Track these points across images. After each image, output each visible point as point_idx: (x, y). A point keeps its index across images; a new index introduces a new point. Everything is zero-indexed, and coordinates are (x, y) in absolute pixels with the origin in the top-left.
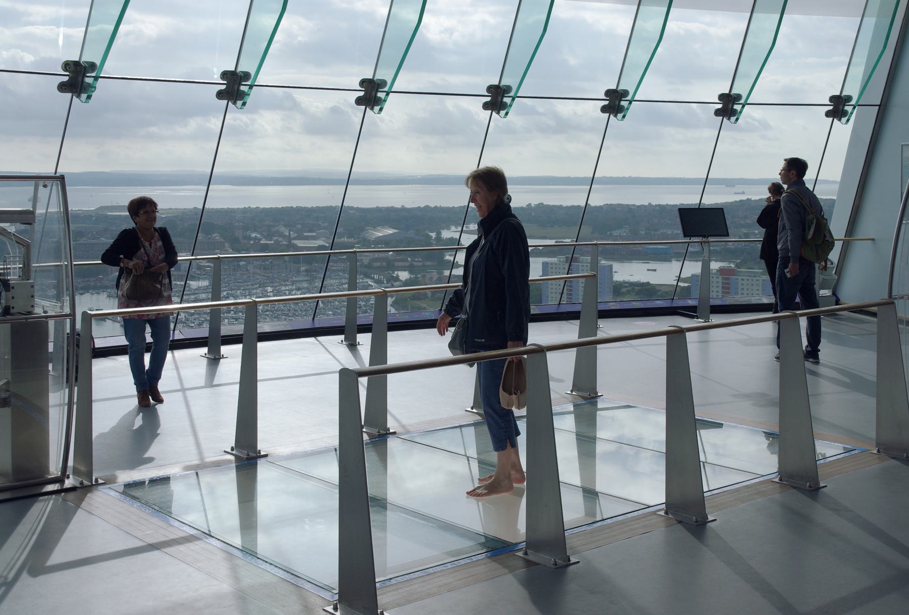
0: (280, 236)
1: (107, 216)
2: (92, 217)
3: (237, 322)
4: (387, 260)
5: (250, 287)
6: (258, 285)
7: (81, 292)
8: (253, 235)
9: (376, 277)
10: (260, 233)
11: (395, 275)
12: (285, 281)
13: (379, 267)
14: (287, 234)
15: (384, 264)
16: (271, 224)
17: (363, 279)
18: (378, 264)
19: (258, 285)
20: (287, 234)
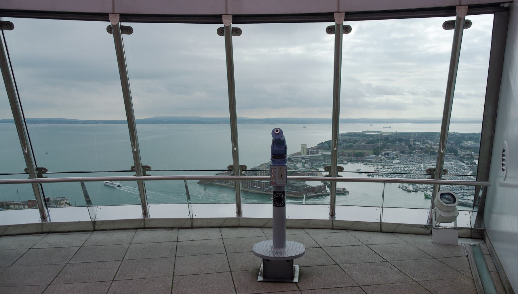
0: (428, 144)
1: (365, 135)
2: (360, 135)
3: (408, 177)
4: (471, 155)
5: (414, 164)
6: (418, 163)
7: (355, 162)
8: (417, 143)
9: (466, 162)
10: (420, 142)
11: (473, 161)
12: (428, 162)
13: (467, 158)
14: (430, 143)
15: (470, 157)
16: (425, 139)
17: (460, 162)
18: (467, 157)
19: (418, 163)
20: (430, 143)
